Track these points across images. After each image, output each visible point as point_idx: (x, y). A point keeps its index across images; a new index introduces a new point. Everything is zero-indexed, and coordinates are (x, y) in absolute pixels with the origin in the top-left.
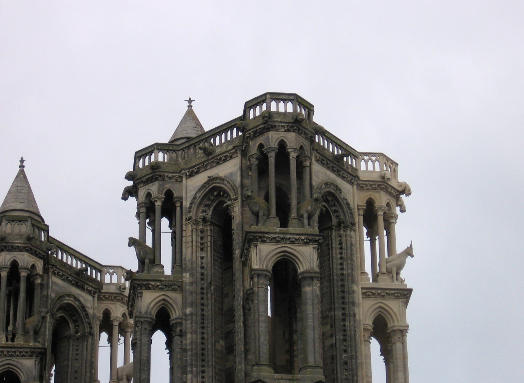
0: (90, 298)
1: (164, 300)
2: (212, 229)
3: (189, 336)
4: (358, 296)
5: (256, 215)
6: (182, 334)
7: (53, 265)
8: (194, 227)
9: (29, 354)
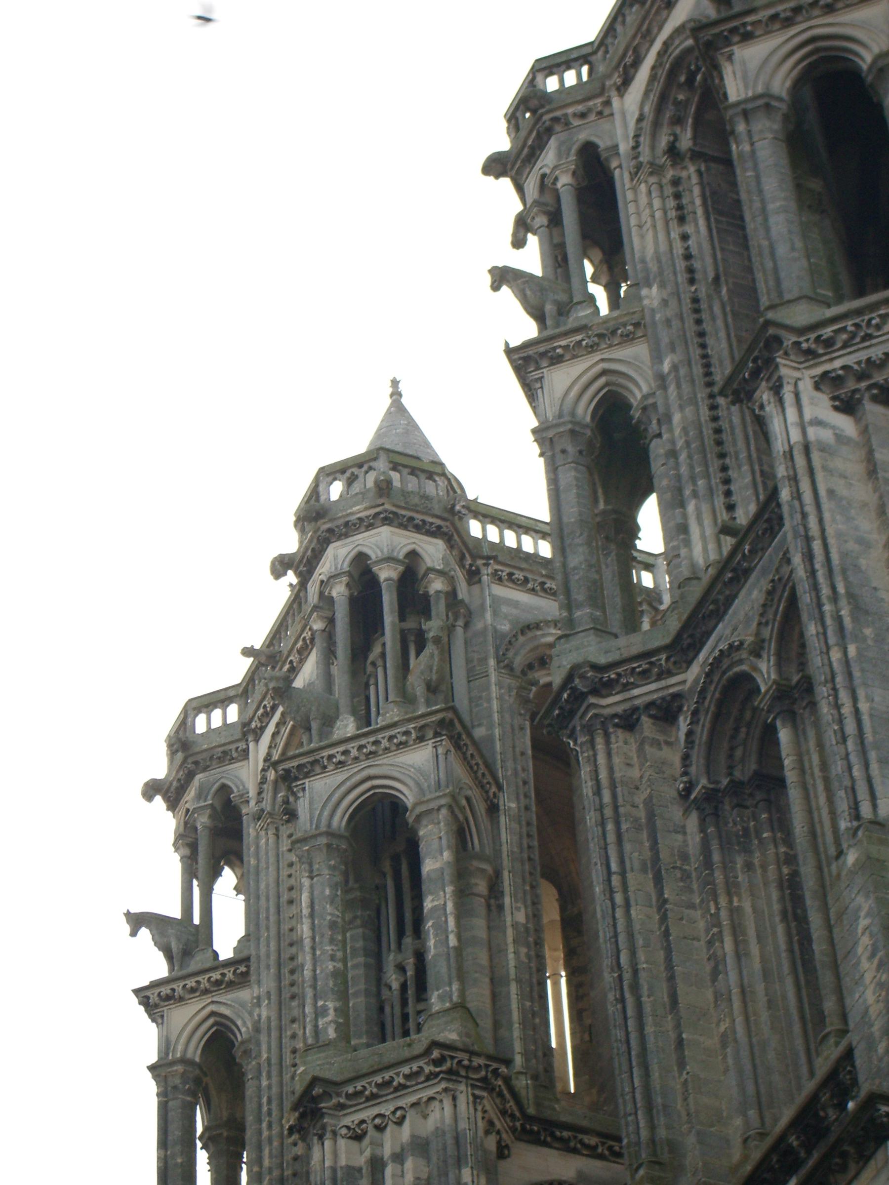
1: (604, 372)
2: (703, 169)
3: (677, 418)
7: (488, 558)
8: (652, 180)
9: (414, 736)
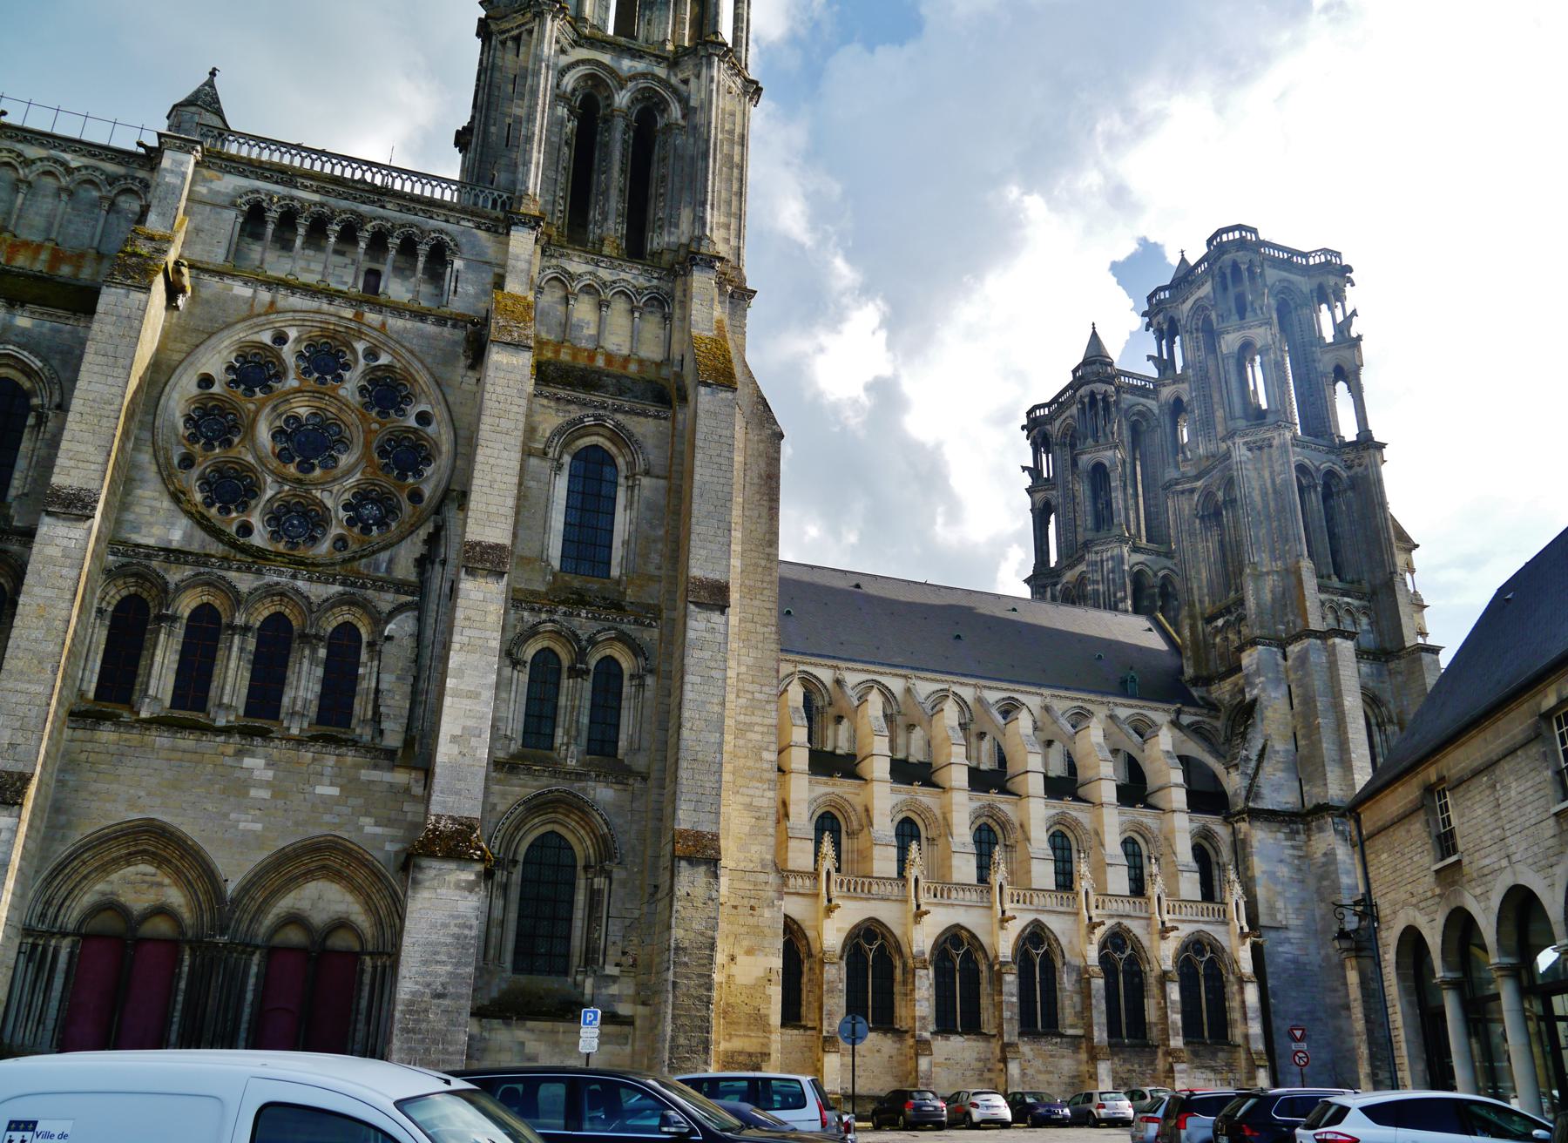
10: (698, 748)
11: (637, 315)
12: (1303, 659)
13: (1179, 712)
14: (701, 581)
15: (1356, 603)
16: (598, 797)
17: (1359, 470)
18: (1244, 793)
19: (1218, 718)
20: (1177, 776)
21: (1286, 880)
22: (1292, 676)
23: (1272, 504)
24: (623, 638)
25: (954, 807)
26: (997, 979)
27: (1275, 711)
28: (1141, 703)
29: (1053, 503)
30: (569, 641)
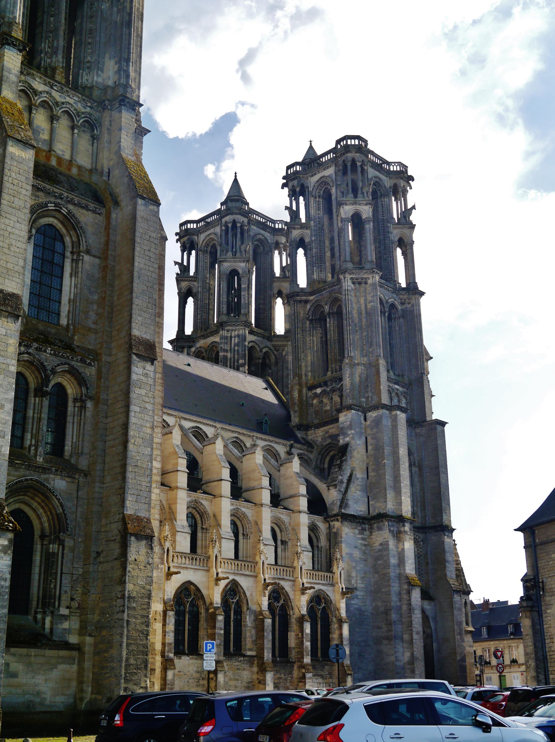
0: (269, 235)
3: (314, 250)
4: (391, 229)
5: (343, 193)
6: (311, 249)
10: (138, 458)
11: (76, 131)
12: (377, 422)
13: (291, 446)
14: (139, 339)
15: (401, 389)
16: (56, 486)
17: (409, 306)
18: (339, 503)
19: (312, 452)
20: (303, 490)
21: (358, 559)
22: (369, 431)
23: (364, 320)
24: (73, 372)
25: (178, 501)
26: (212, 618)
27: (358, 453)
28: (271, 438)
29: (194, 290)
30: (37, 369)
